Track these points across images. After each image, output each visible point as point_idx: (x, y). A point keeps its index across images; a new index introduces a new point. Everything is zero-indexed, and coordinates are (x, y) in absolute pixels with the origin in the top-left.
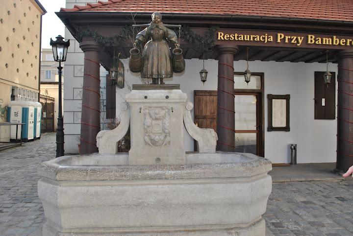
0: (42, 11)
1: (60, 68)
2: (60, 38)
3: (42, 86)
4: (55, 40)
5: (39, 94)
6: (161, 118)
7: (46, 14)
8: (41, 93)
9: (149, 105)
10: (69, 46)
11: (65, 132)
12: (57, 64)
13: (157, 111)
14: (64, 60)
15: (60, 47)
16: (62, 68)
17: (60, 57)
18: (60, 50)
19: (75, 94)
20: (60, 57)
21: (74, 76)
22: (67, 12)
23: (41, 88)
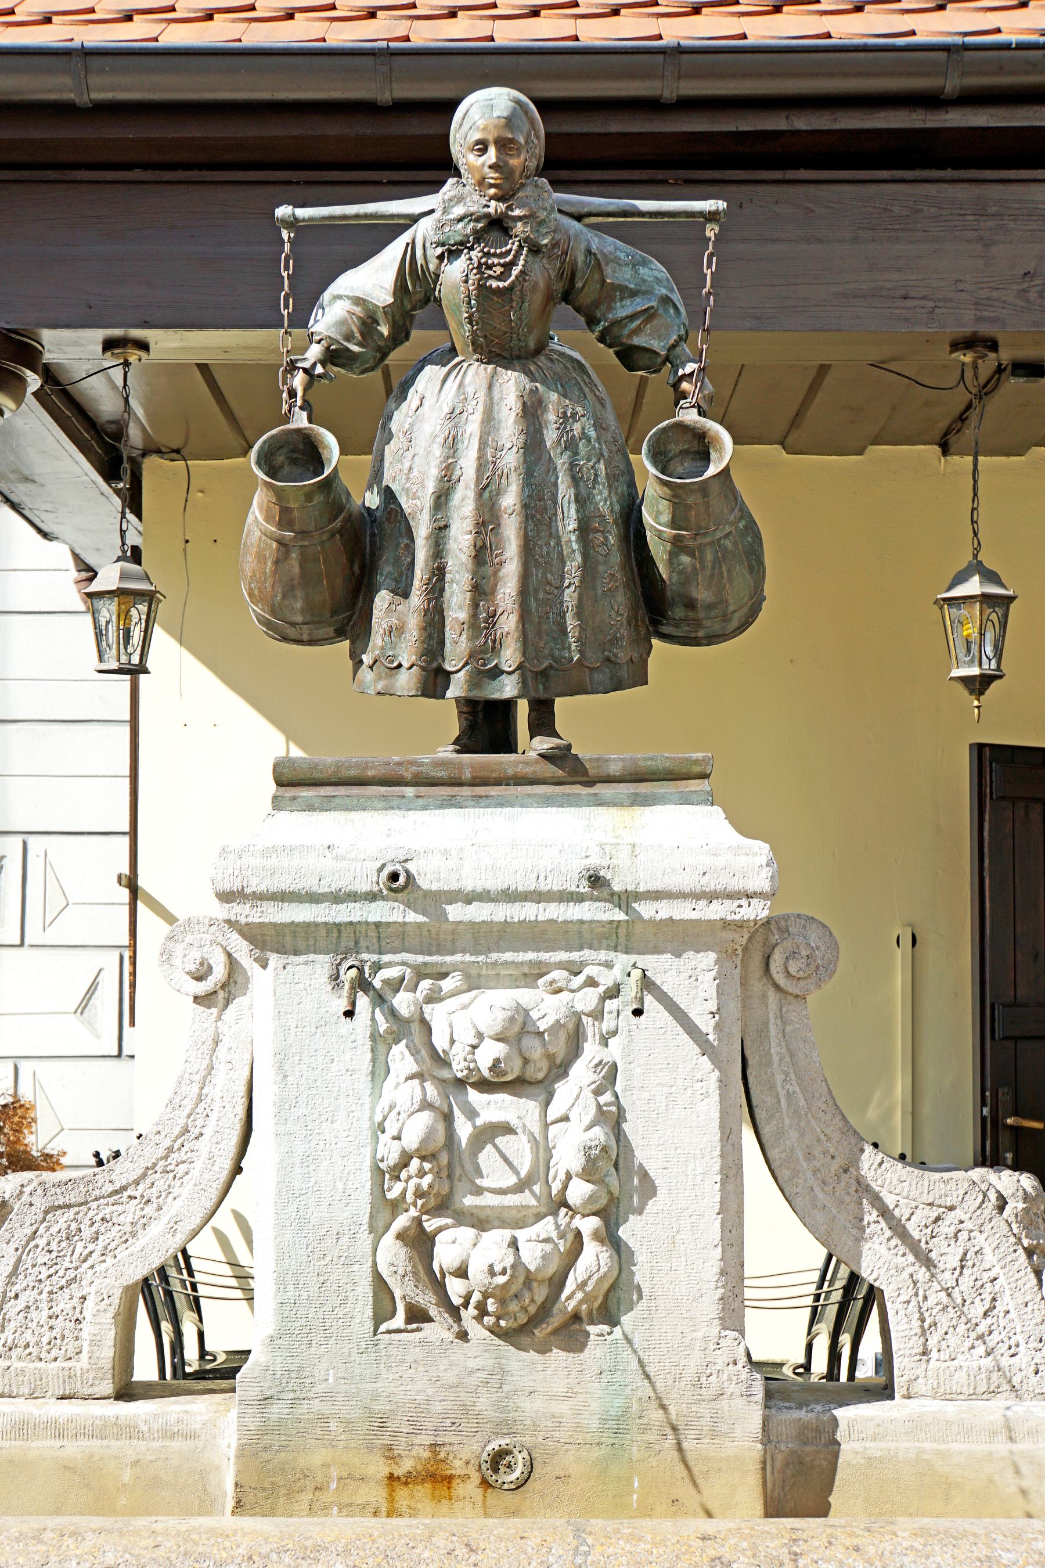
6: (539, 1070)
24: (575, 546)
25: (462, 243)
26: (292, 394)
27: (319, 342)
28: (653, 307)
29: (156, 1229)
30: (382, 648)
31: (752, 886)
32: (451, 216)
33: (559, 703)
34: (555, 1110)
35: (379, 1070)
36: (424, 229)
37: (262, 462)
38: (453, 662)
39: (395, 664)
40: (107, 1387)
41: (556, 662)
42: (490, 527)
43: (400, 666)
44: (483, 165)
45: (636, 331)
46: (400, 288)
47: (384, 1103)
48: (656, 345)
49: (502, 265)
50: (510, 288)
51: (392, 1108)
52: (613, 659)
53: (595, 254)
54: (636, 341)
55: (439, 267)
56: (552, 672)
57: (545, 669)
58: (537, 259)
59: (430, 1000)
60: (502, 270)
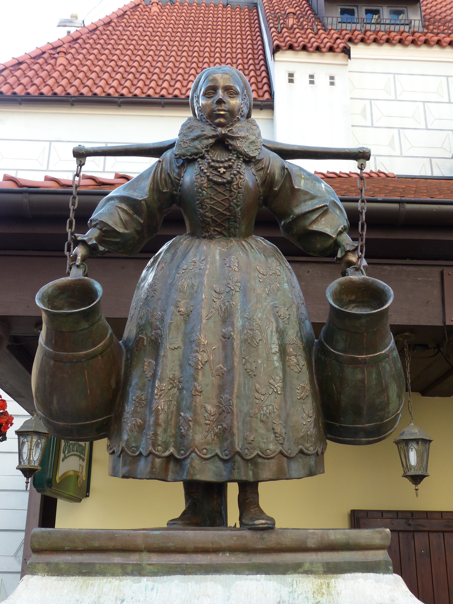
24: (277, 364)
25: (196, 154)
26: (75, 258)
27: (95, 226)
28: (326, 206)
30: (127, 441)
32: (190, 138)
33: (261, 486)
37: (46, 300)
38: (182, 452)
39: (137, 453)
41: (262, 453)
42: (214, 348)
43: (141, 454)
44: (213, 102)
45: (314, 222)
48: (328, 231)
49: (225, 168)
50: (230, 183)
52: (306, 451)
53: (287, 169)
54: (315, 227)
55: (179, 175)
56: (260, 460)
57: (253, 458)
58: (249, 168)
60: (225, 170)
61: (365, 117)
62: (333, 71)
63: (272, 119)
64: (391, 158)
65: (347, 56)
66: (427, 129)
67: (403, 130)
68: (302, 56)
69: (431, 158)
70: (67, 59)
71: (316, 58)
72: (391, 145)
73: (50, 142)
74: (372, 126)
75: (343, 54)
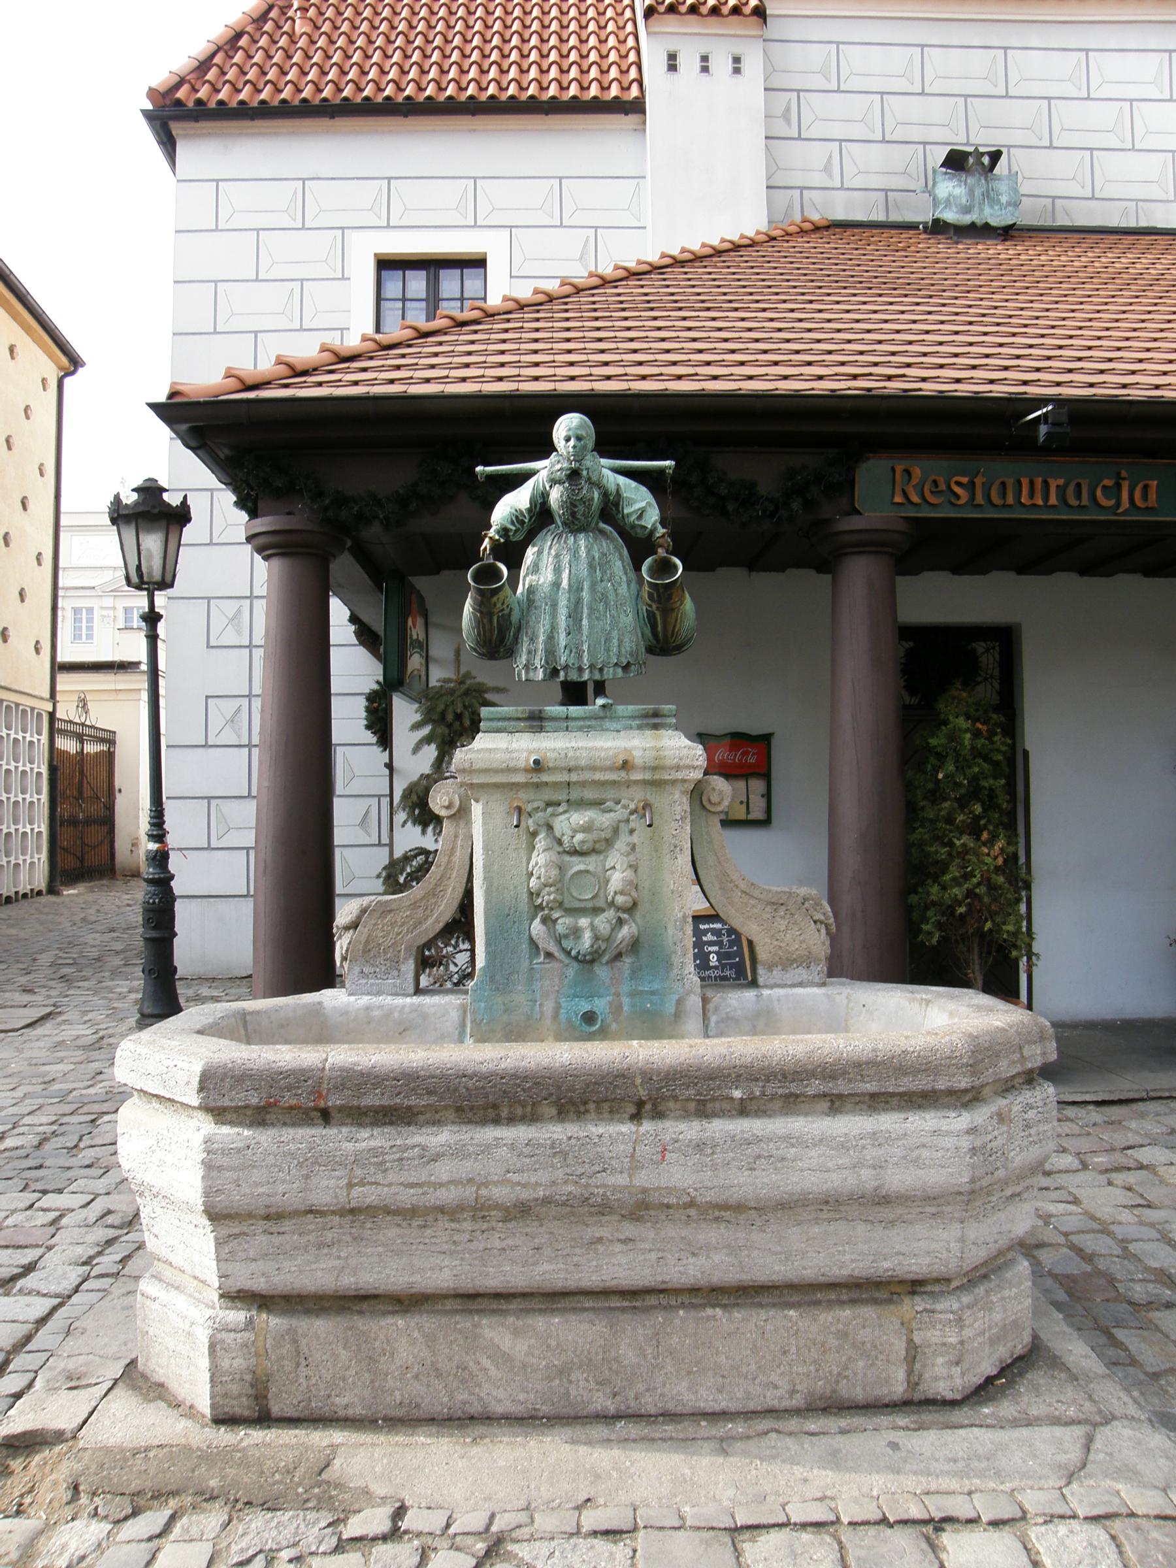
0: (64, 361)
1: (152, 618)
2: (150, 491)
3: (66, 682)
4: (130, 498)
5: (52, 715)
7: (81, 370)
8: (58, 715)
9: (548, 795)
10: (188, 520)
11: (177, 886)
12: (140, 601)
13: (579, 818)
14: (166, 583)
15: (149, 531)
16: (158, 617)
17: (153, 567)
18: (152, 542)
19: (216, 722)
20: (153, 567)
21: (208, 646)
22: (198, 403)
23: (59, 688)
29: (430, 921)
31: (696, 763)
34: (609, 863)
35: (532, 847)
36: (542, 476)
40: (412, 990)
46: (533, 500)
47: (532, 863)
51: (537, 864)
59: (553, 815)
61: (788, 121)
62: (738, 48)
63: (644, 130)
64: (827, 192)
65: (761, 21)
66: (884, 141)
67: (849, 144)
68: (693, 25)
69: (886, 191)
70: (311, 20)
71: (714, 26)
72: (827, 169)
73: (304, 180)
74: (799, 138)
75: (755, 18)
